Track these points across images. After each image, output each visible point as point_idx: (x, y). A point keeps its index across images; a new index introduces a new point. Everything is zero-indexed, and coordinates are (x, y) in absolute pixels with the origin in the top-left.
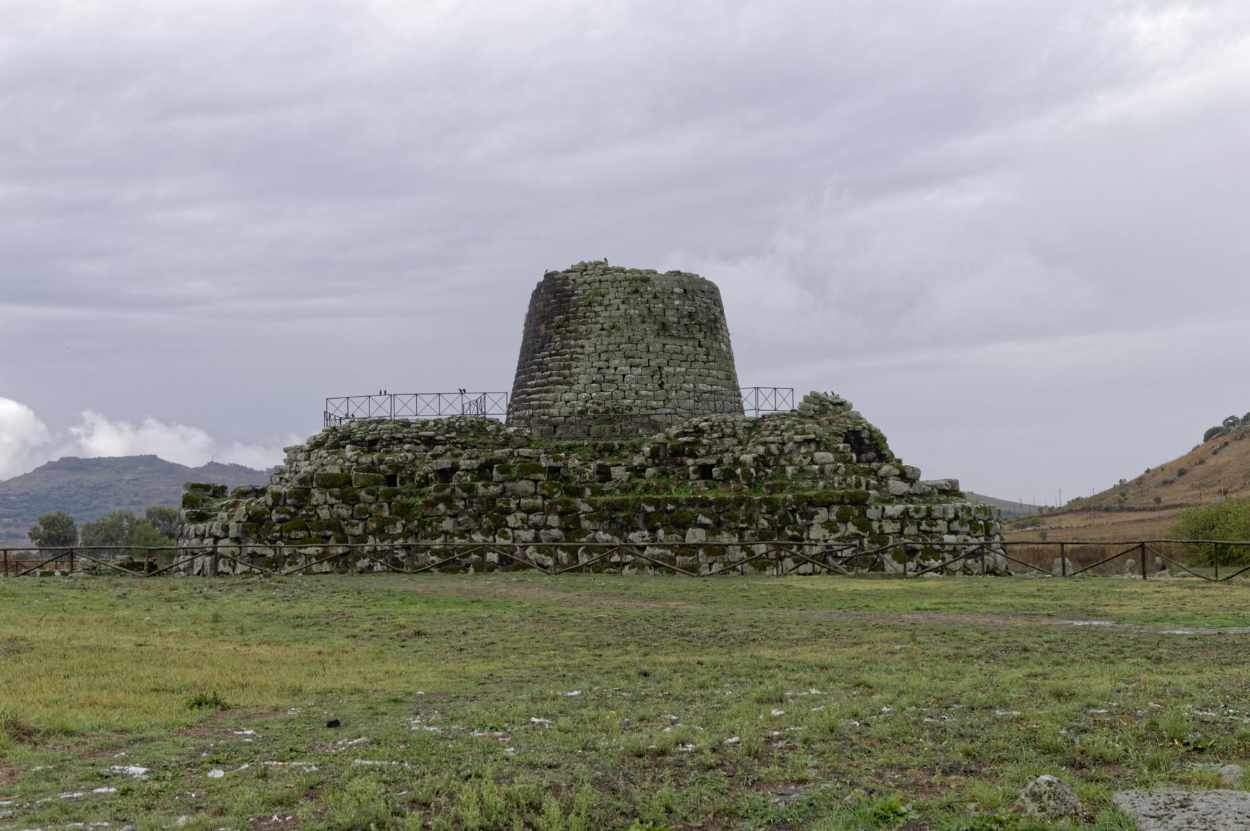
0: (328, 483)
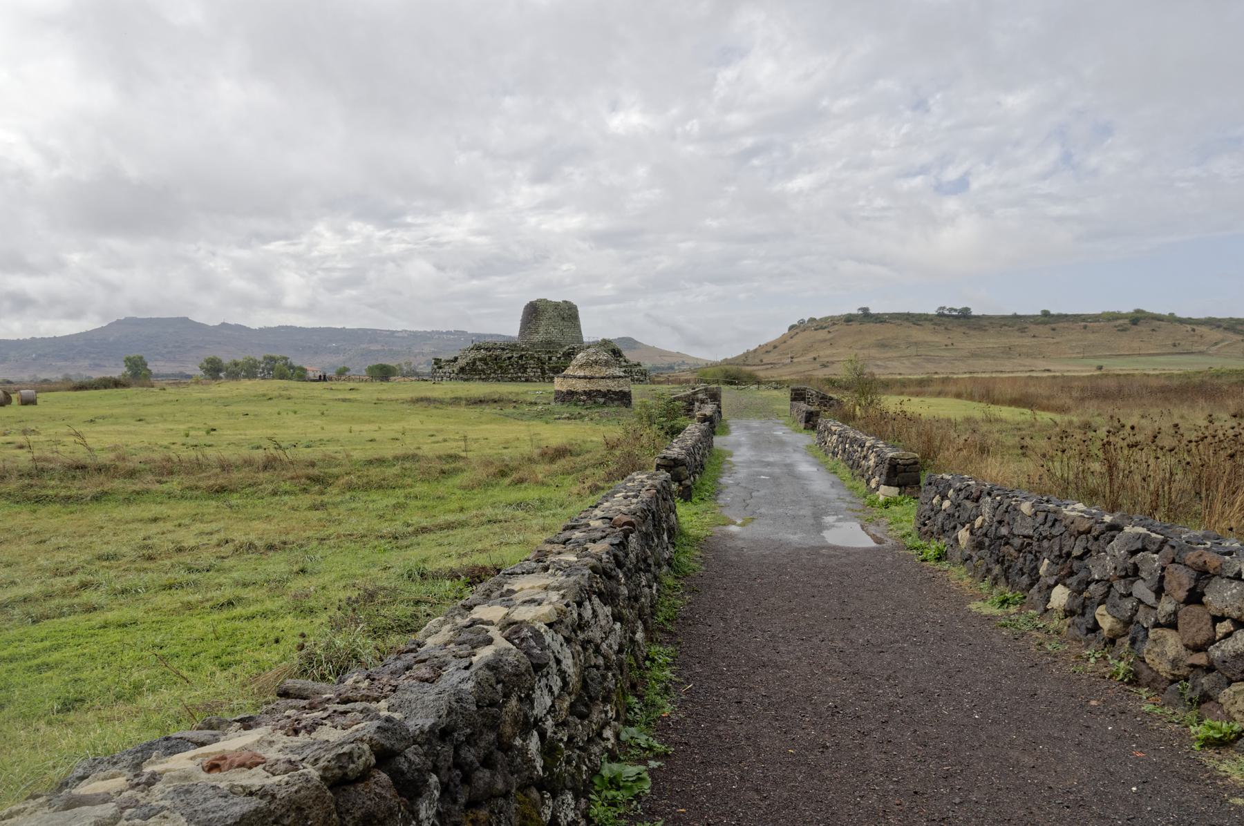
0: (480, 360)
